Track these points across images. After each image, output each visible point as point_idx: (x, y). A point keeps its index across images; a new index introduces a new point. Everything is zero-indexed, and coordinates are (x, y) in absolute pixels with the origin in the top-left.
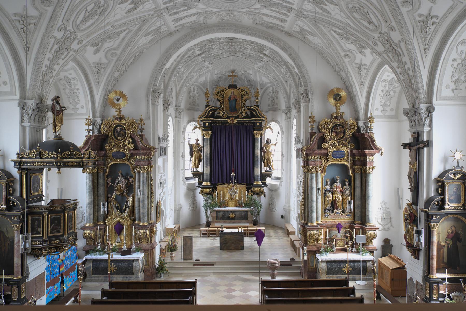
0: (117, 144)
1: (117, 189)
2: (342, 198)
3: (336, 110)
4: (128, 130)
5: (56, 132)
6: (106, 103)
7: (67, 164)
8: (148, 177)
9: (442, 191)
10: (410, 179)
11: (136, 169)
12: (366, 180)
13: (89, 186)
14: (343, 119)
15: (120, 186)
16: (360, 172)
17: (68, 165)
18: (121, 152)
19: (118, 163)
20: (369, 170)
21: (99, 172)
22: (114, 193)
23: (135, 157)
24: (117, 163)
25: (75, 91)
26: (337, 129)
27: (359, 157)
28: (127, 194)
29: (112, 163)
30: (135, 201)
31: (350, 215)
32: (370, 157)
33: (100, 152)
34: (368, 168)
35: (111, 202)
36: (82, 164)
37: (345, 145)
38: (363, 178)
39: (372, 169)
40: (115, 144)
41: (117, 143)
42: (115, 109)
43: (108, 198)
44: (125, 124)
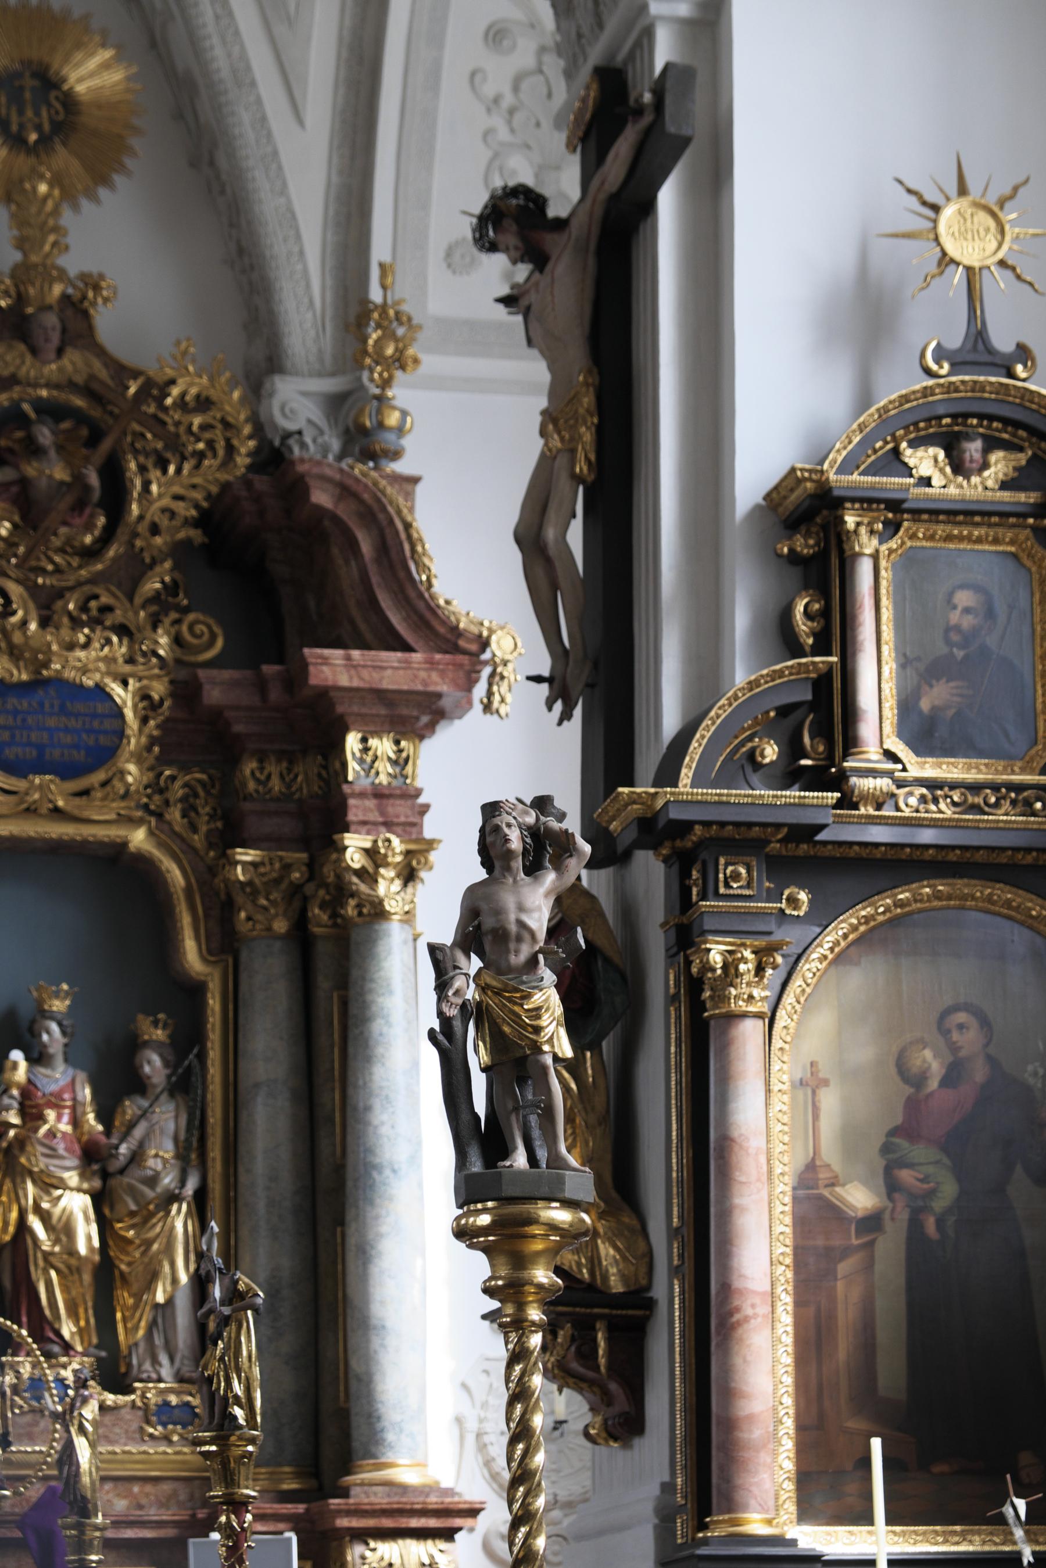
2: (104, 1225)
3: (21, 243)
9: (825, 613)
10: (540, 572)
12: (344, 1004)
14: (101, 352)
16: (281, 926)
20: (368, 876)
26: (35, 451)
27: (273, 768)
31: (186, 1416)
32: (383, 746)
34: (354, 858)
37: (123, 631)
38: (323, 984)
39: (409, 876)
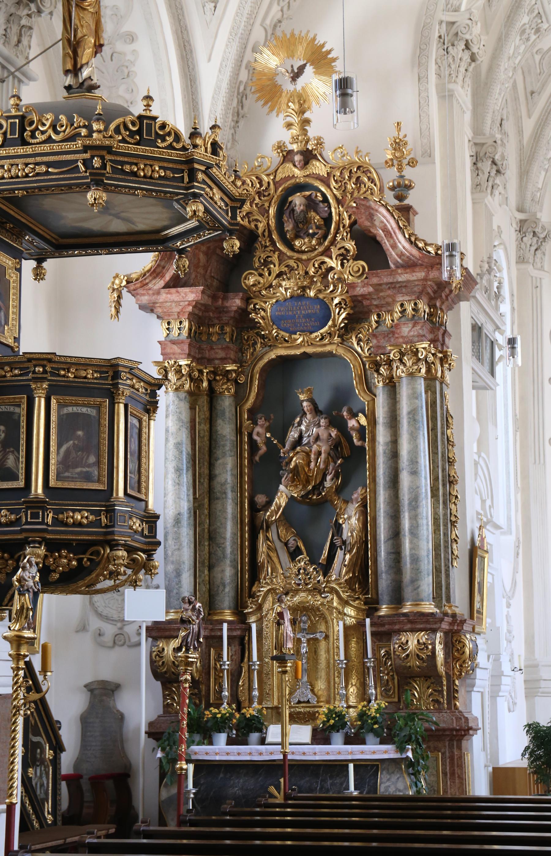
0: (291, 269)
1: (296, 471)
4: (339, 202)
5: (76, 70)
6: (241, 103)
7: (127, 168)
8: (434, 403)
11: (377, 371)
13: (178, 445)
15: (308, 454)
17: (135, 174)
18: (310, 298)
19: (298, 352)
21: (218, 389)
22: (282, 487)
23: (374, 318)
24: (292, 352)
25: (120, 46)
28: (339, 490)
29: (272, 355)
30: (374, 519)
33: (225, 298)
35: (268, 527)
36: (186, 179)
40: (284, 269)
41: (292, 263)
42: (281, 116)
43: (254, 509)
44: (325, 181)
